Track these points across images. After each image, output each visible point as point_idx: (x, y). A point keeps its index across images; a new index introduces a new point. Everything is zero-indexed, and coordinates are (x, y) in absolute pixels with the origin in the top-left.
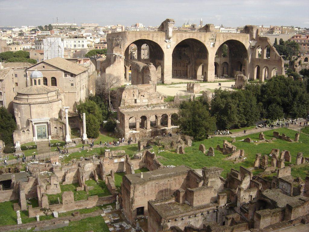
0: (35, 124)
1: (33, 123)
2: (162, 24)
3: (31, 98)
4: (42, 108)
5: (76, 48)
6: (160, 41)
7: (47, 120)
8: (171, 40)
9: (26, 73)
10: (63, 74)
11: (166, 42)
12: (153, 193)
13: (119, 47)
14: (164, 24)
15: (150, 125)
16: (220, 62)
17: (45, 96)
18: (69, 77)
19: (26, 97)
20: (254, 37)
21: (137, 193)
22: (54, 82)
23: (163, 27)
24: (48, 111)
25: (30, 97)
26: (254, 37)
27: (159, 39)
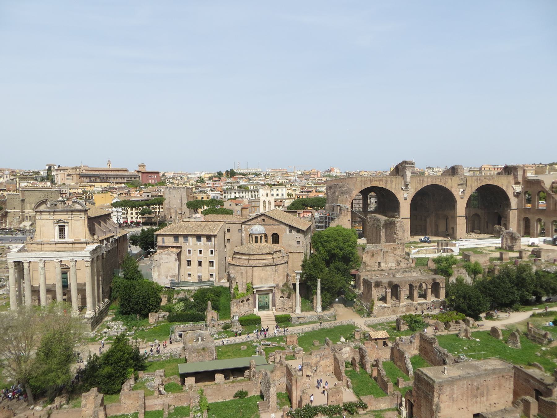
1: (255, 290)
2: (397, 168)
4: (267, 271)
6: (395, 188)
7: (272, 287)
10: (288, 229)
14: (400, 168)
16: (469, 213)
17: (270, 257)
18: (294, 233)
19: (247, 257)
20: (520, 179)
21: (444, 398)
22: (276, 239)
23: (399, 170)
24: (273, 275)
26: (520, 179)
27: (394, 186)
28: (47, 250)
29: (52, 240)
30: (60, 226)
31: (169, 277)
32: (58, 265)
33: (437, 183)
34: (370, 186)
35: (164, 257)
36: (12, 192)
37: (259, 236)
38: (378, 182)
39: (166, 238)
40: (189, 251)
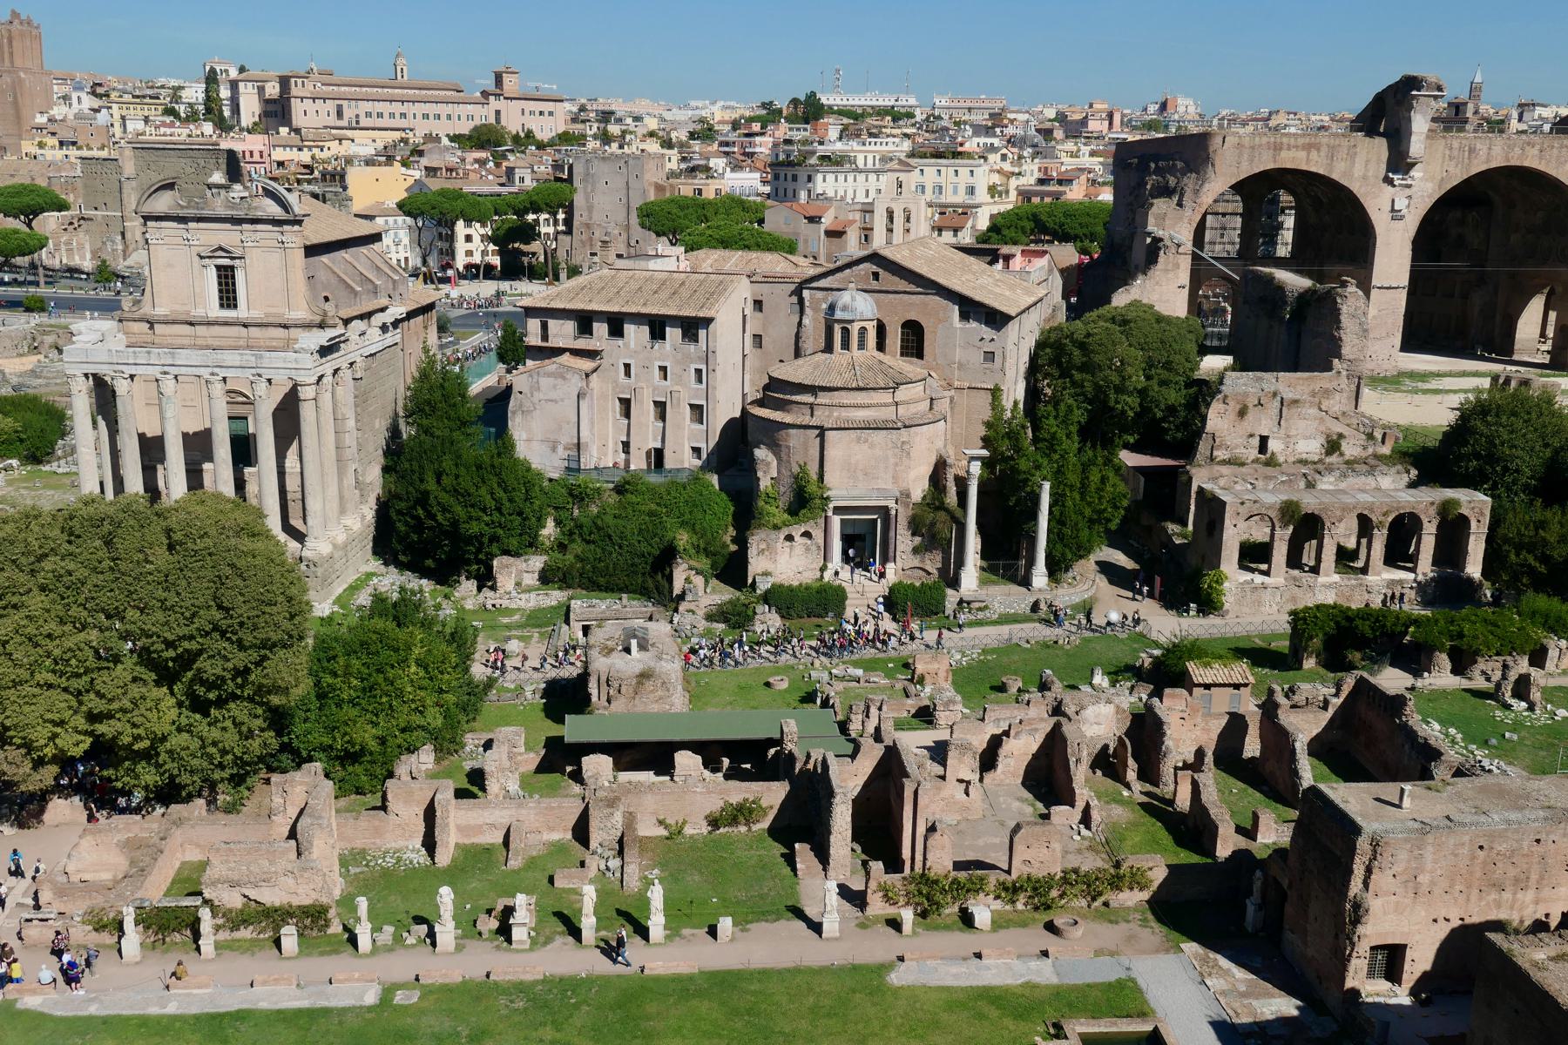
0: (837, 510)
1: (831, 506)
3: (827, 401)
4: (872, 446)
5: (943, 200)
6: (1365, 177)
8: (1416, 173)
9: (801, 302)
11: (1390, 182)
12: (1458, 888)
13: (1176, 199)
15: (1333, 558)
17: (886, 397)
22: (914, 340)
23: (1385, 116)
24: (892, 461)
25: (823, 398)
27: (1358, 170)
28: (179, 341)
29: (198, 313)
30: (218, 268)
31: (560, 449)
32: (218, 389)
33: (1526, 164)
34: (1270, 166)
35: (545, 382)
36: (95, 153)
37: (855, 329)
38: (1303, 154)
39: (552, 323)
40: (627, 366)
